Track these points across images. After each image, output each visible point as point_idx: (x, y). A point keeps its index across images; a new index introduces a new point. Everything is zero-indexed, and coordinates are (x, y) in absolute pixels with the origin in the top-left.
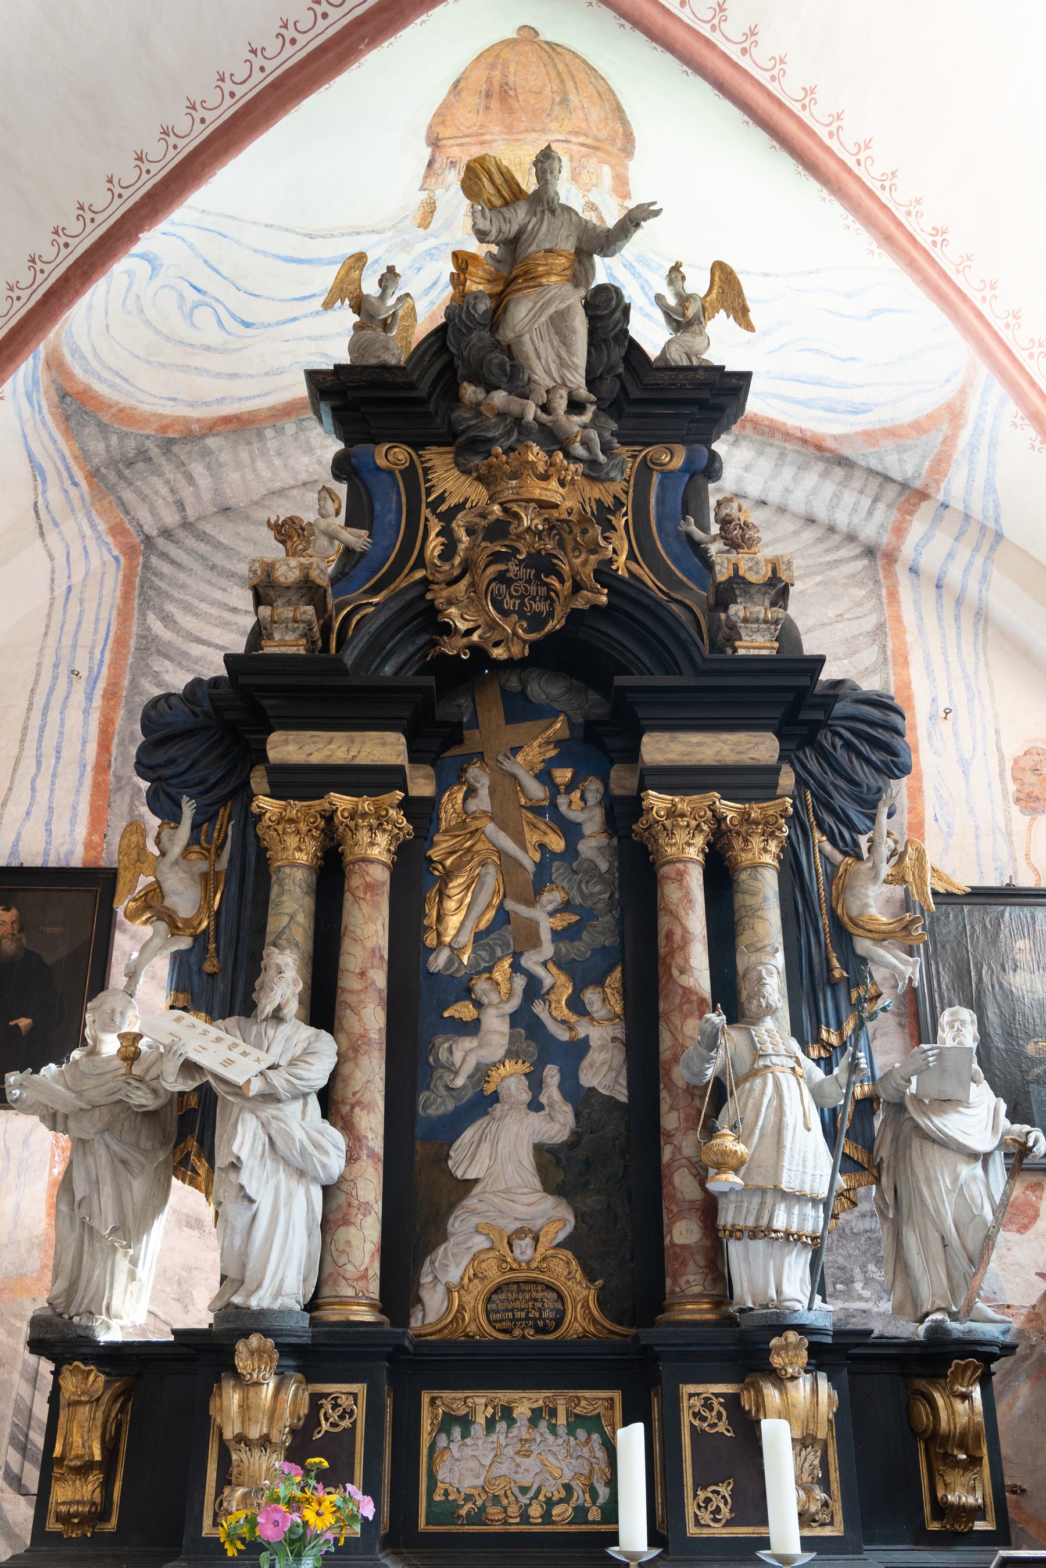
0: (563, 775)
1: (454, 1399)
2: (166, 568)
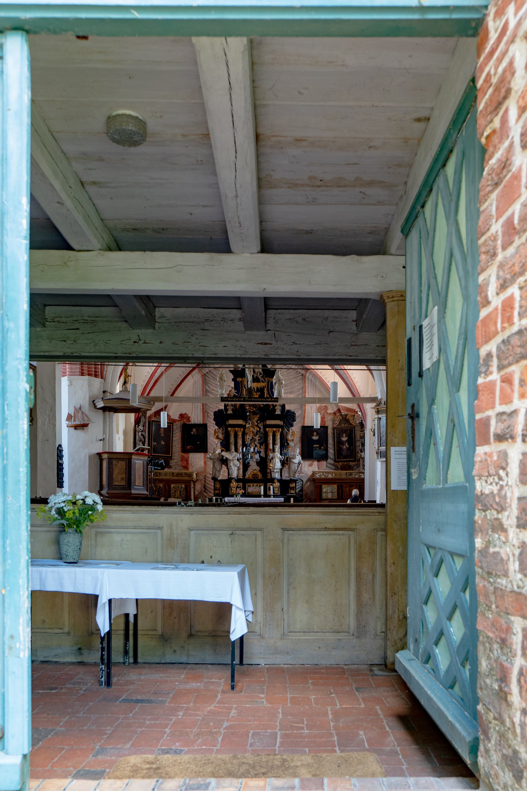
0: (259, 422)
1: (249, 484)
2: (208, 378)
